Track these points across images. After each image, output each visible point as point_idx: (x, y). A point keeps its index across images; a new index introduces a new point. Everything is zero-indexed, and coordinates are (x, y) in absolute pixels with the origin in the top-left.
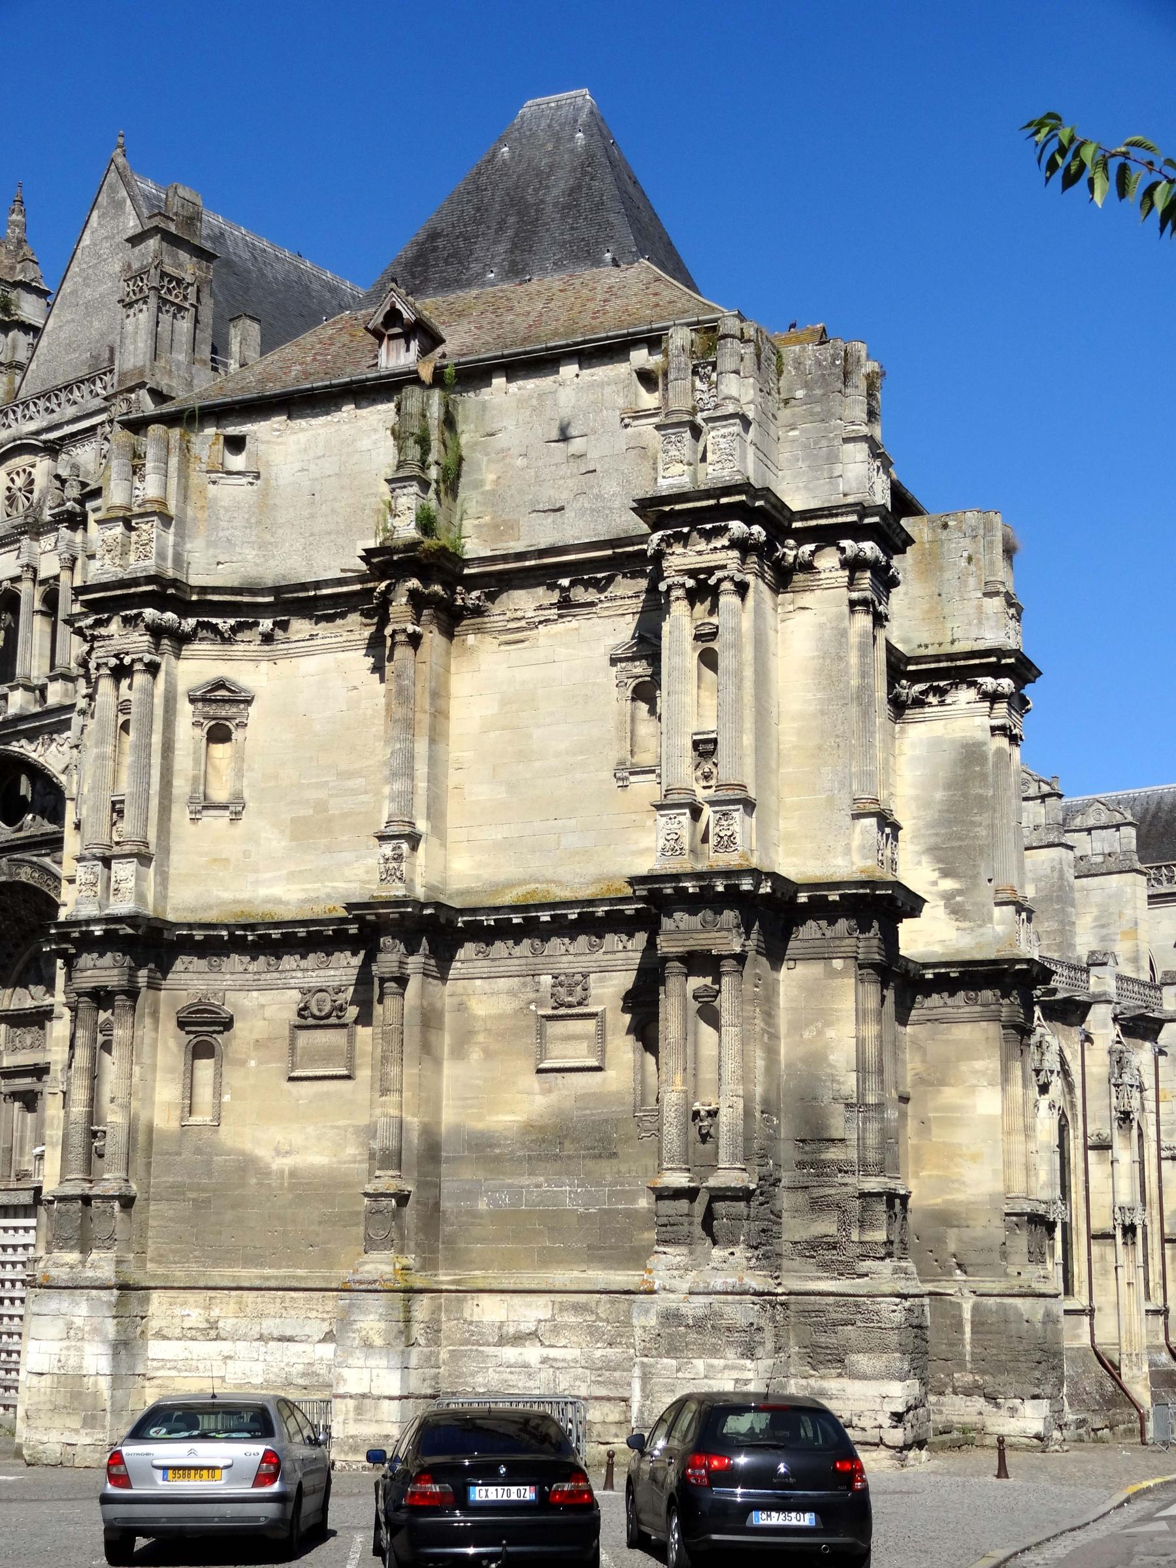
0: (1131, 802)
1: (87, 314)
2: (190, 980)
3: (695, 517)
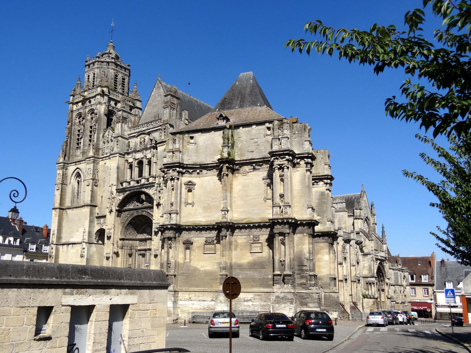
0: (343, 198)
2: (185, 235)
3: (280, 155)
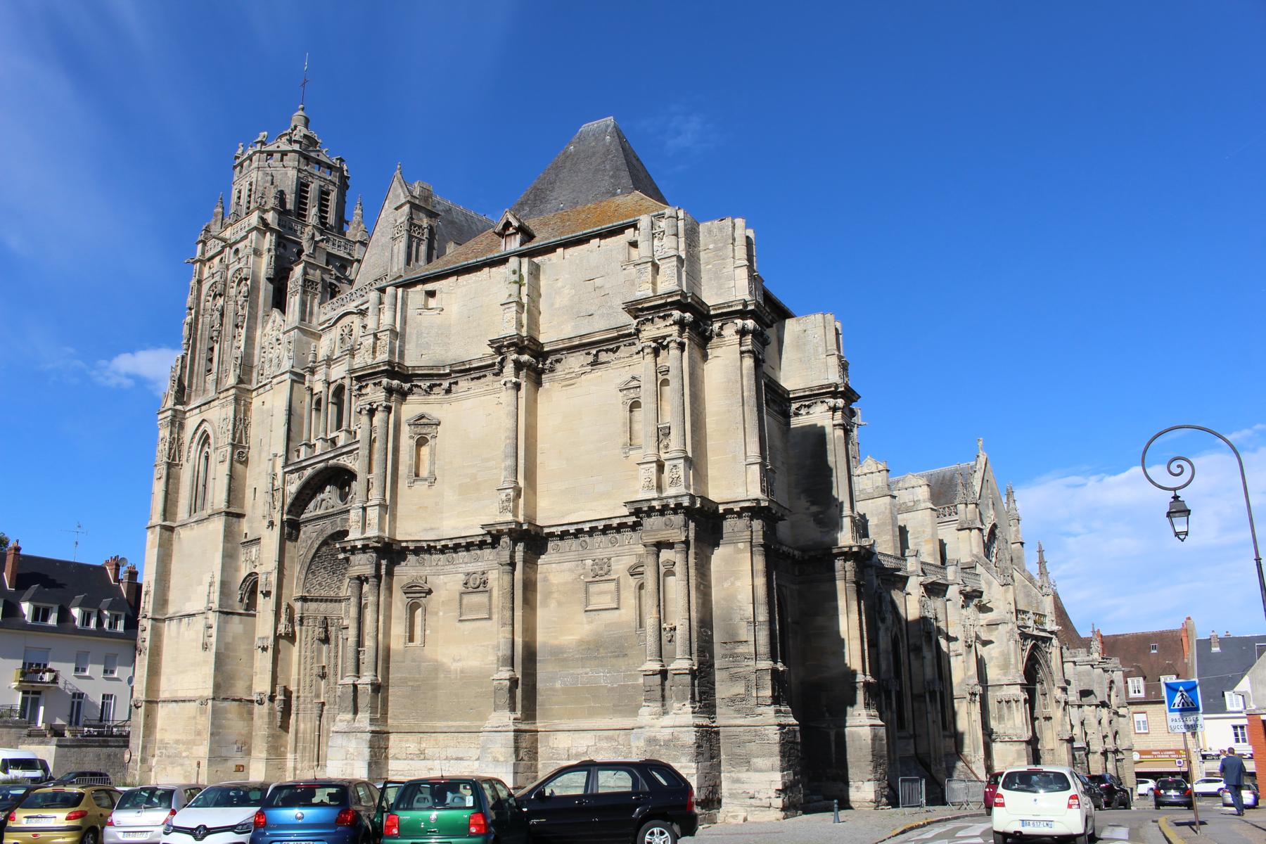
2: (406, 572)
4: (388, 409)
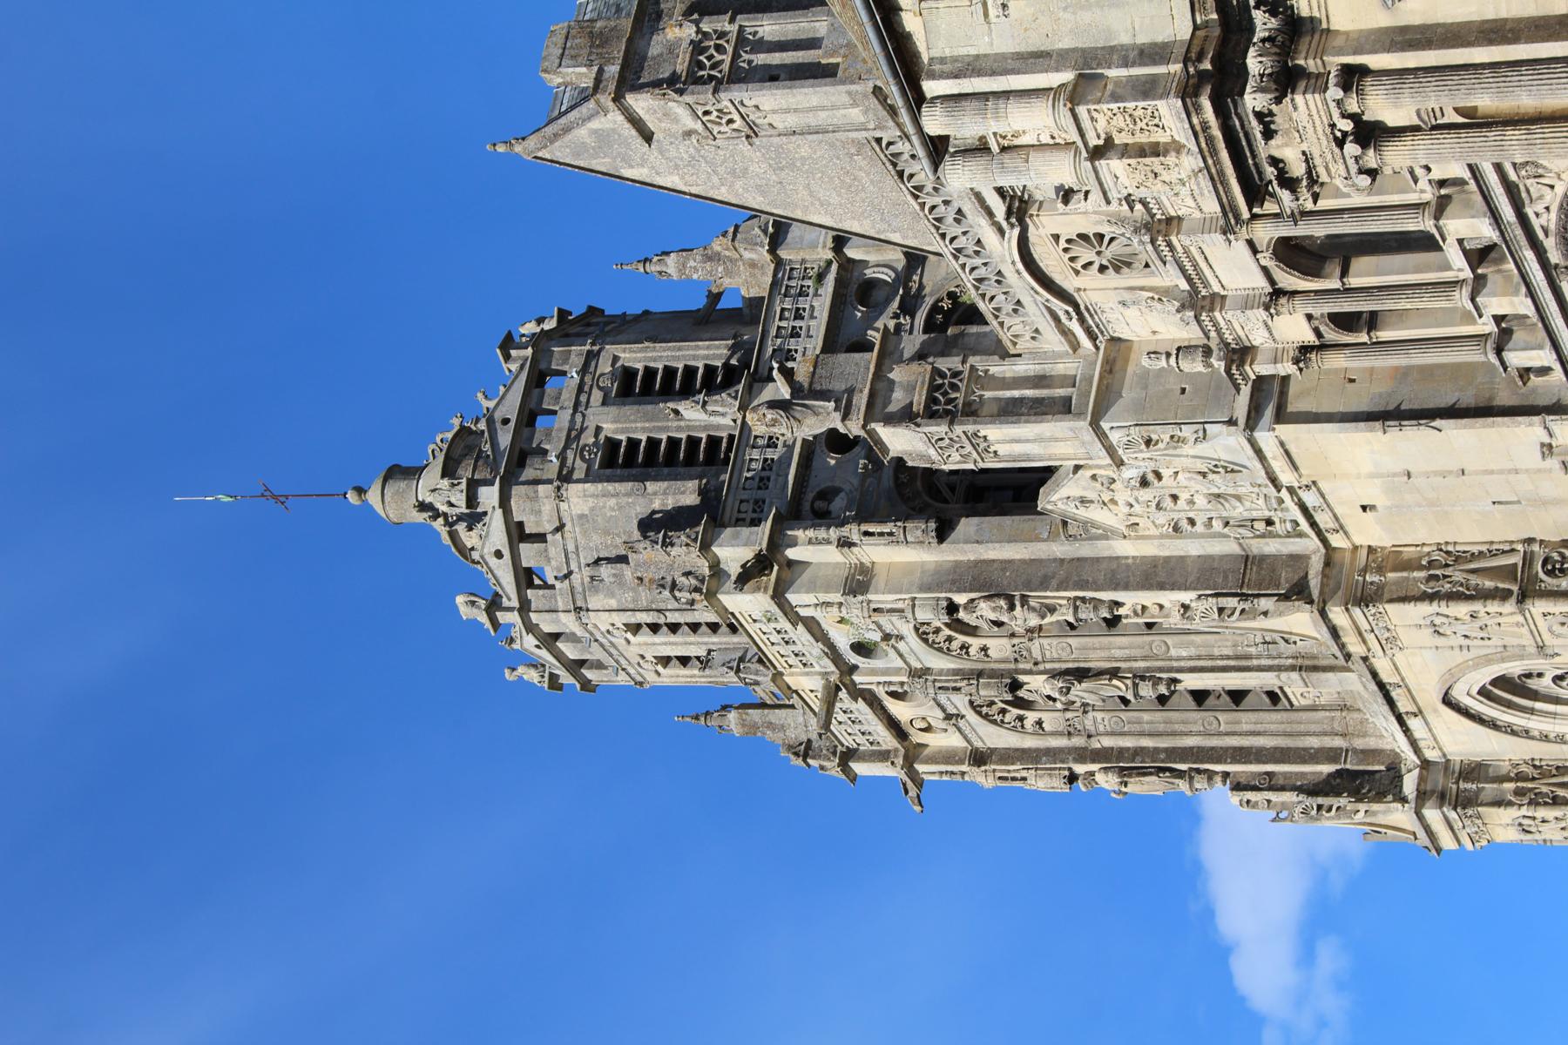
1: (792, 166)
4: (1352, 77)
